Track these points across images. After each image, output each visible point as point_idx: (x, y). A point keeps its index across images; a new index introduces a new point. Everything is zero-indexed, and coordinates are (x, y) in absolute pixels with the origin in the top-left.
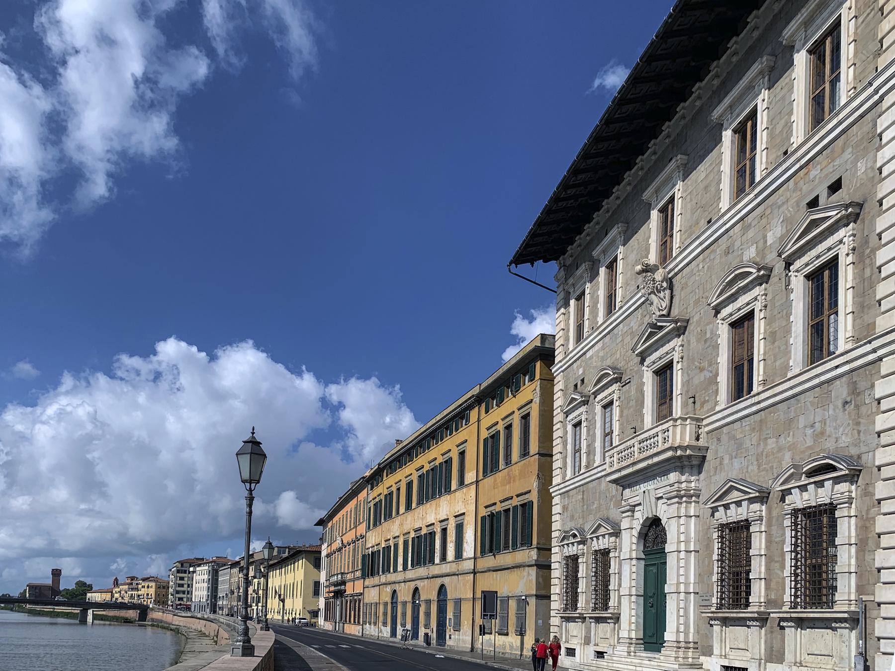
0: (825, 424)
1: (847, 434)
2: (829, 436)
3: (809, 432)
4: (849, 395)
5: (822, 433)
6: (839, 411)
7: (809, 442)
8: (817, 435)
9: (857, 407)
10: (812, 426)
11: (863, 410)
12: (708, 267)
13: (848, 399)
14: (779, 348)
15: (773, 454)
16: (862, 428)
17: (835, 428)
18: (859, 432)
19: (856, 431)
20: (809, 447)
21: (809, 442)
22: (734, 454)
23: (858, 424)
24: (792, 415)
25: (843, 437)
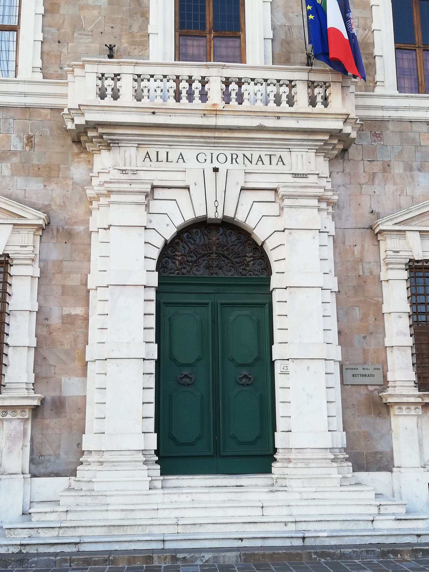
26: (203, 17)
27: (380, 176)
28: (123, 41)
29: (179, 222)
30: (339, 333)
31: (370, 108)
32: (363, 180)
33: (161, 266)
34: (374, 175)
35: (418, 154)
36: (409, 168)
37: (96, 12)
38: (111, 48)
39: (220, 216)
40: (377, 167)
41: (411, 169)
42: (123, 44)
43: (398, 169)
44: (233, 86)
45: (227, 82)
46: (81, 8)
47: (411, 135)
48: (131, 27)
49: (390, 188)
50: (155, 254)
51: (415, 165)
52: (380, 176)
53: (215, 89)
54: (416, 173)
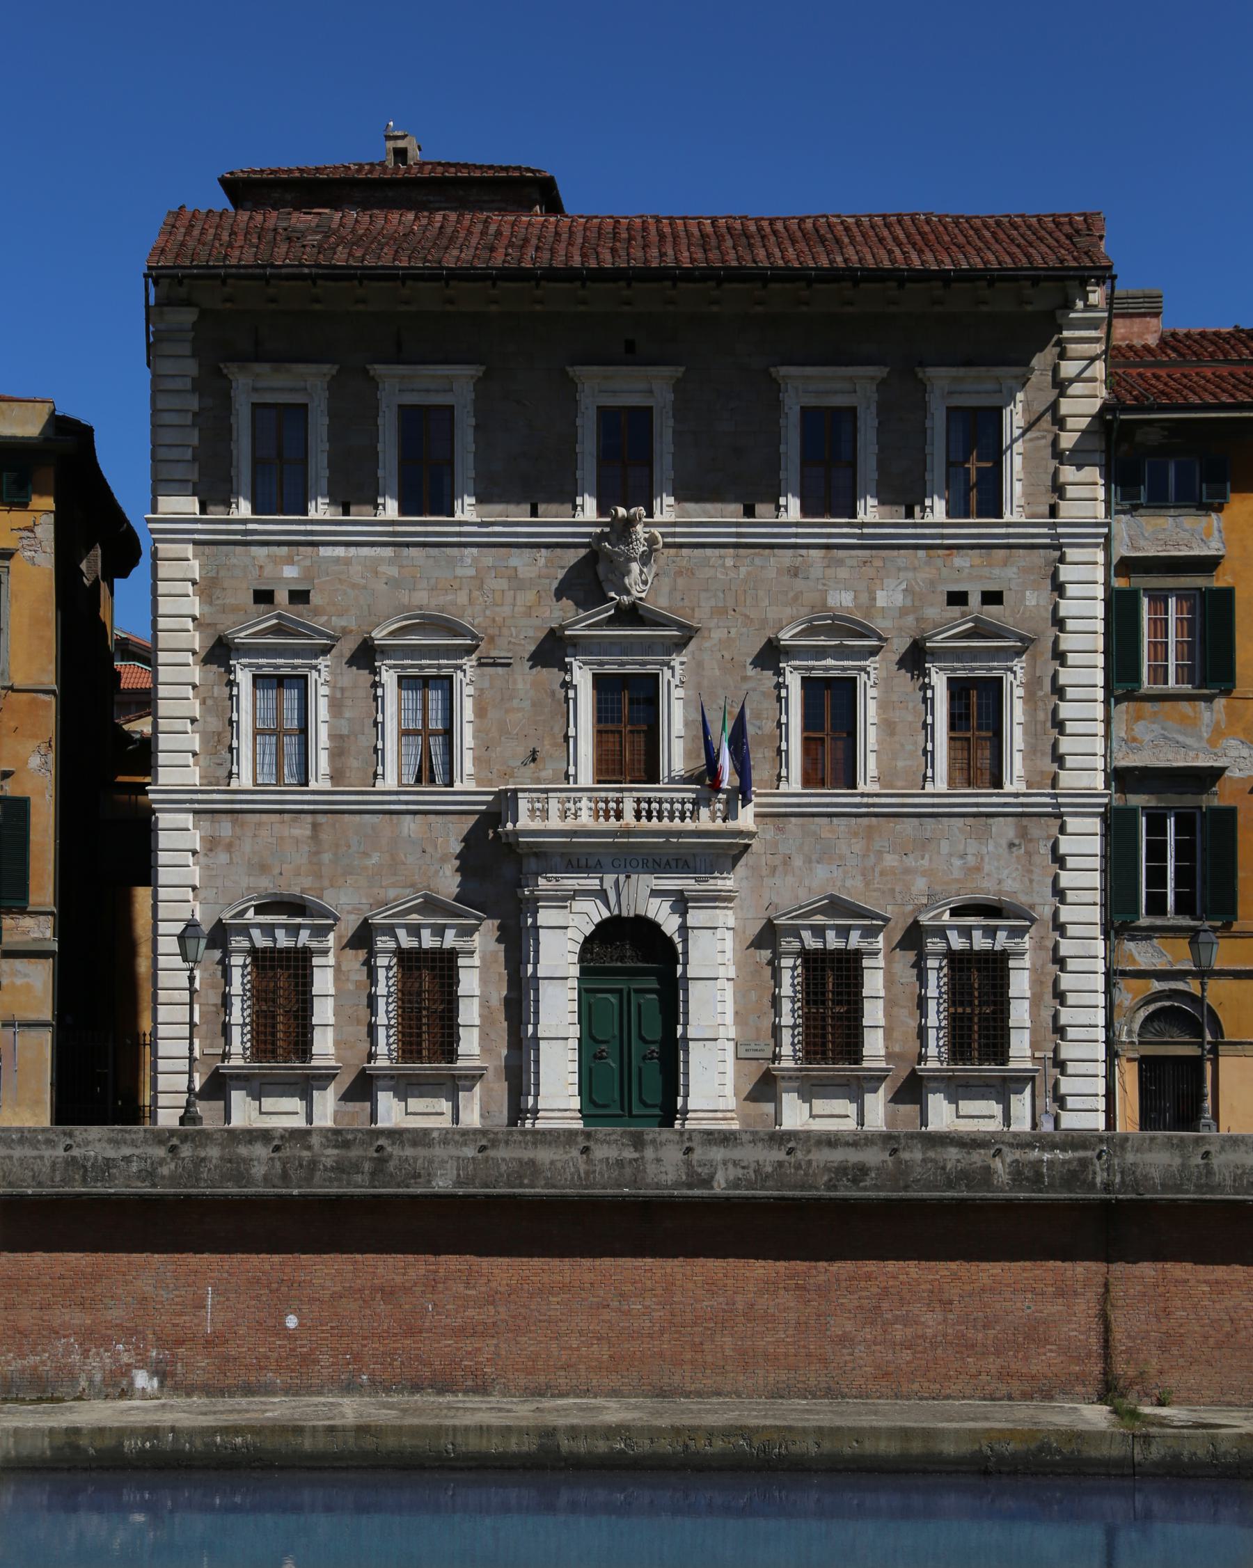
0: (982, 859)
1: (1014, 879)
2: (988, 875)
3: (957, 863)
4: (1017, 837)
5: (978, 869)
6: (1003, 850)
7: (957, 874)
8: (969, 869)
9: (1029, 854)
10: (963, 856)
11: (1037, 859)
12: (749, 573)
13: (1017, 842)
14: (902, 745)
15: (895, 874)
16: (1035, 877)
17: (998, 868)
18: (1031, 881)
19: (1026, 879)
20: (957, 880)
21: (957, 874)
22: (814, 857)
23: (1030, 872)
24: (928, 835)
25: (1010, 881)
26: (620, 710)
27: (780, 868)
28: (546, 743)
29: (597, 920)
30: (736, 1013)
31: (715, 899)
32: (764, 873)
33: (581, 960)
34: (775, 867)
35: (818, 847)
36: (808, 860)
37: (520, 715)
38: (534, 752)
39: (632, 915)
40: (777, 860)
41: (810, 862)
42: (545, 748)
43: (798, 862)
44: (644, 805)
45: (638, 801)
46: (507, 711)
47: (813, 827)
48: (552, 728)
49: (790, 880)
50: (577, 949)
51: (814, 857)
52: (780, 868)
53: (629, 807)
54: (814, 865)
